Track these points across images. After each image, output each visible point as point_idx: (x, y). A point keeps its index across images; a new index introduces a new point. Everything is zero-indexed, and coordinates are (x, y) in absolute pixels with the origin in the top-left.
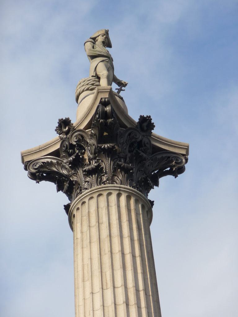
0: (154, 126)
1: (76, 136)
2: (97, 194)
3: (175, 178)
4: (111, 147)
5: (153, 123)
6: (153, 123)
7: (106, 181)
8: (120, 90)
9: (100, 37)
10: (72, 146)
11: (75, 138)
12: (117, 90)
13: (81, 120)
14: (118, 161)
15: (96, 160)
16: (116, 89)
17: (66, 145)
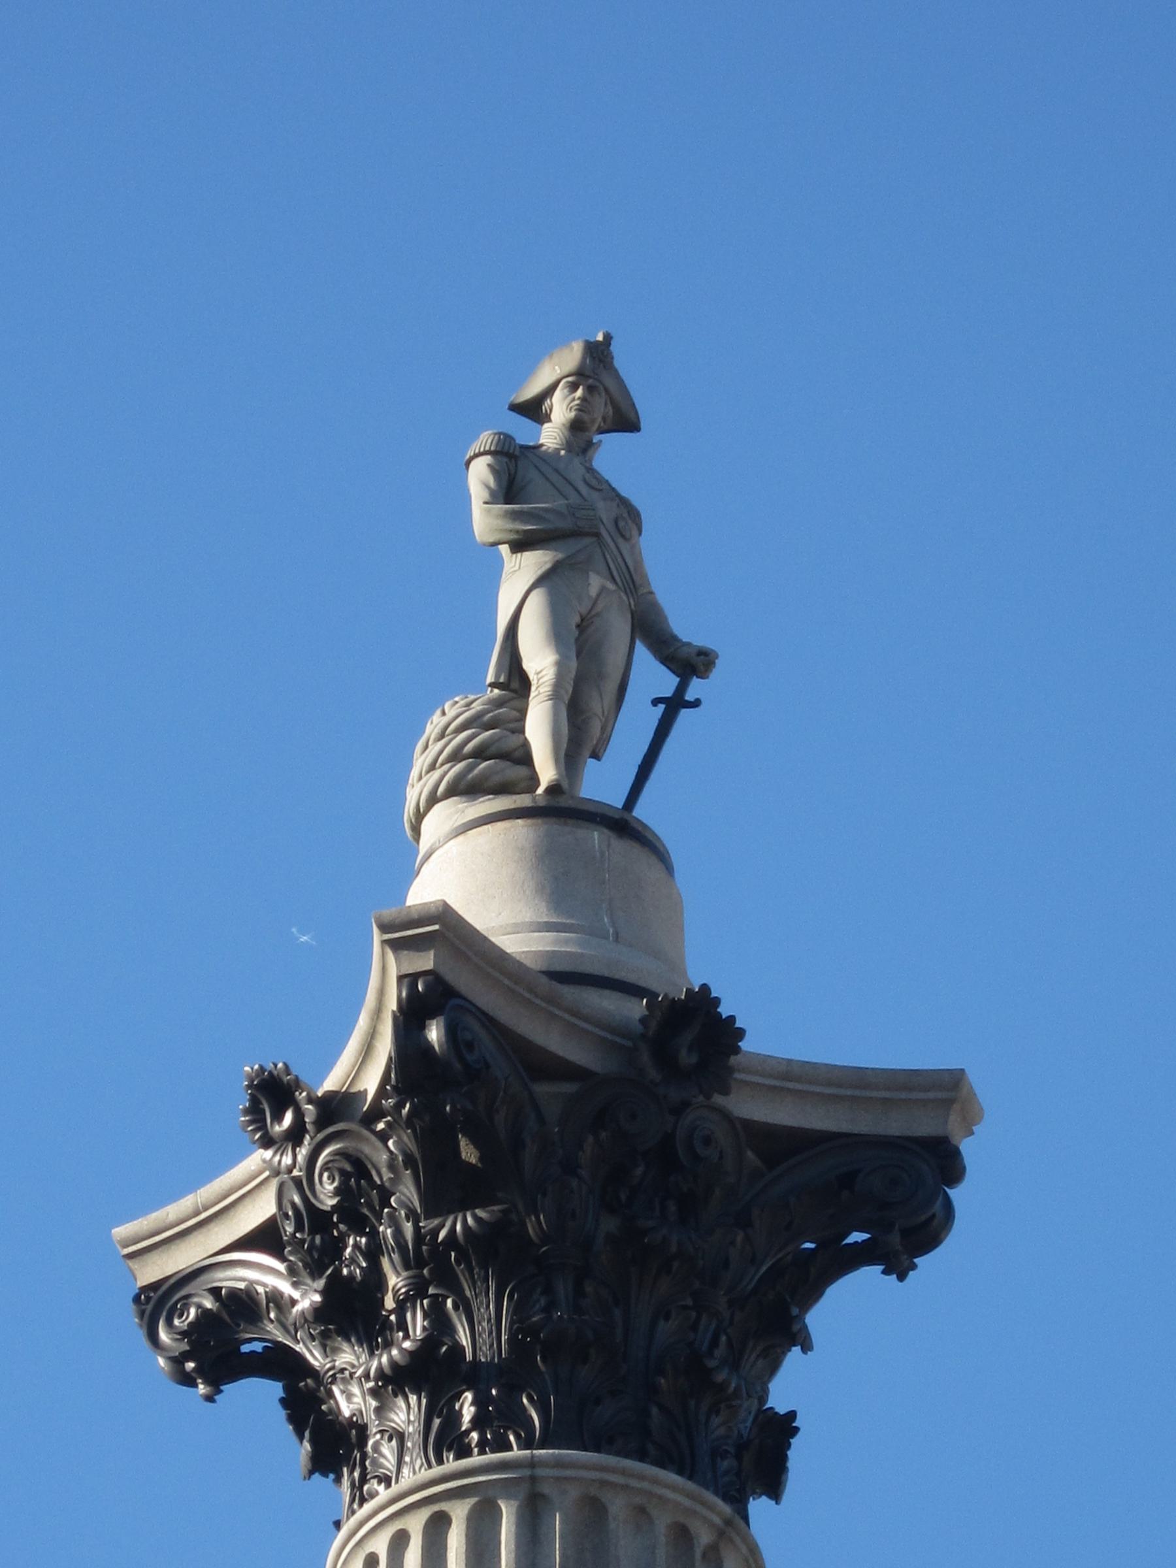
0: (740, 1034)
1: (325, 1167)
2: (424, 1514)
3: (902, 1277)
4: (500, 1215)
5: (732, 1019)
6: (732, 1019)
7: (468, 1432)
8: (674, 705)
9: (558, 394)
10: (315, 1219)
11: (326, 1175)
12: (662, 707)
13: (354, 1067)
14: (539, 1290)
15: (425, 1302)
16: (656, 702)
17: (294, 1205)
